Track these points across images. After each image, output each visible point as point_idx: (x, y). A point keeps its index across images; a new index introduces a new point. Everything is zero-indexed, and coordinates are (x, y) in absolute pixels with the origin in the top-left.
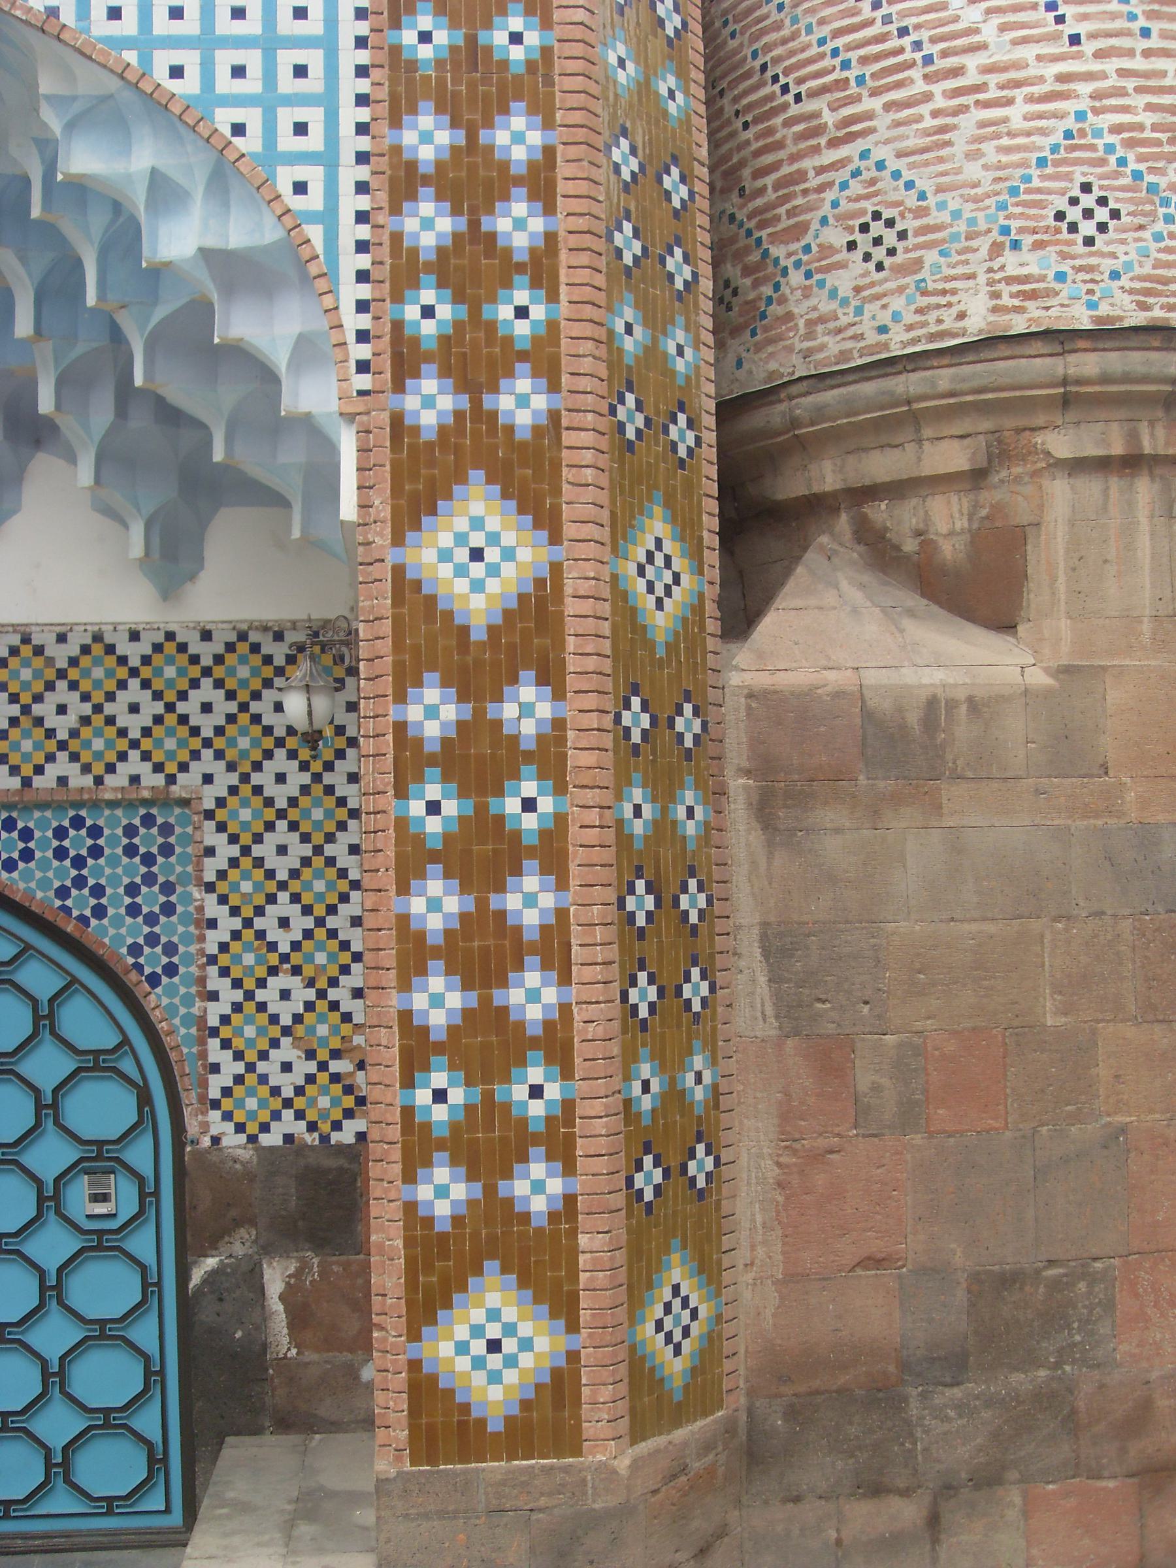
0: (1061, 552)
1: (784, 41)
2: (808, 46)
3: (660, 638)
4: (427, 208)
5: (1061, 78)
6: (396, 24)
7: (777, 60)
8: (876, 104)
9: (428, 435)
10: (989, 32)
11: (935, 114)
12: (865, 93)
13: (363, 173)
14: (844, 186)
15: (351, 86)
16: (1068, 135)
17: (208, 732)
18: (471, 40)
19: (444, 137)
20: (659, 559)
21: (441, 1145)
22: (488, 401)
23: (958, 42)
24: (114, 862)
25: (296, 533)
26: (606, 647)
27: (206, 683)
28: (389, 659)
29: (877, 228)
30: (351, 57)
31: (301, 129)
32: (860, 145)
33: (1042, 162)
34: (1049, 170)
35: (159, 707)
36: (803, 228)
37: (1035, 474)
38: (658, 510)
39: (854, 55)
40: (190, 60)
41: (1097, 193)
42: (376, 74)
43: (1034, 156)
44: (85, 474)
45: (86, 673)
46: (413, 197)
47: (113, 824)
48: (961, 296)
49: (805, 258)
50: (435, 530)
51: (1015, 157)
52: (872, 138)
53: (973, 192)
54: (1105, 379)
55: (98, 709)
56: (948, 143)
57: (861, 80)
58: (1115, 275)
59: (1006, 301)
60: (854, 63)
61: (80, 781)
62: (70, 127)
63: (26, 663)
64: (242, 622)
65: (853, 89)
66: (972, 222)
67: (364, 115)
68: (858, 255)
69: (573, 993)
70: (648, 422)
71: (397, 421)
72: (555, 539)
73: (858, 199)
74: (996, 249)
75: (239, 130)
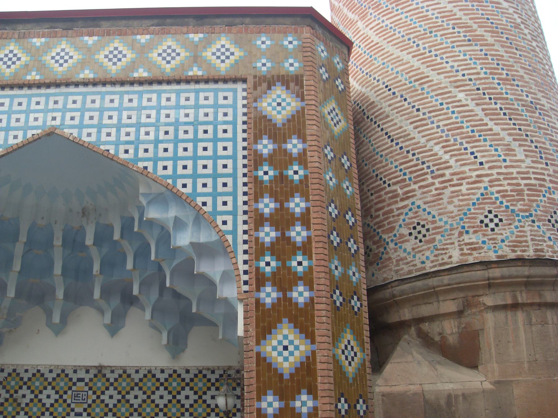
0: (492, 339)
1: (383, 167)
2: (391, 168)
3: (351, 376)
4: (267, 229)
5: (478, 176)
6: (256, 169)
7: (381, 173)
8: (416, 187)
9: (268, 306)
10: (452, 162)
11: (436, 189)
12: (412, 183)
13: (246, 217)
14: (407, 214)
16: (482, 194)
17: (187, 406)
18: (281, 174)
19: (272, 205)
20: (349, 348)
22: (289, 294)
23: (442, 166)
25: (220, 337)
26: (332, 380)
27: (187, 388)
28: (255, 386)
29: (419, 228)
31: (225, 203)
32: (411, 200)
33: (474, 204)
34: (477, 206)
36: (393, 228)
37: (481, 311)
38: (348, 330)
39: (407, 171)
41: (494, 213)
42: (250, 185)
43: (471, 202)
44: (148, 315)
45: (145, 384)
46: (263, 225)
48: (450, 250)
49: (394, 239)
50: (271, 339)
51: (465, 203)
52: (415, 198)
53: (451, 215)
54: (503, 277)
55: (149, 397)
56: (442, 199)
57: (410, 179)
58: (503, 241)
59: (465, 251)
60: (407, 173)
62: (149, 203)
63: (124, 380)
64: (200, 367)
65: (408, 182)
66: (451, 225)
67: (246, 198)
68: (413, 237)
70: (344, 299)
71: (258, 301)
72: (313, 342)
73: (412, 218)
74: (461, 234)
75: (204, 204)
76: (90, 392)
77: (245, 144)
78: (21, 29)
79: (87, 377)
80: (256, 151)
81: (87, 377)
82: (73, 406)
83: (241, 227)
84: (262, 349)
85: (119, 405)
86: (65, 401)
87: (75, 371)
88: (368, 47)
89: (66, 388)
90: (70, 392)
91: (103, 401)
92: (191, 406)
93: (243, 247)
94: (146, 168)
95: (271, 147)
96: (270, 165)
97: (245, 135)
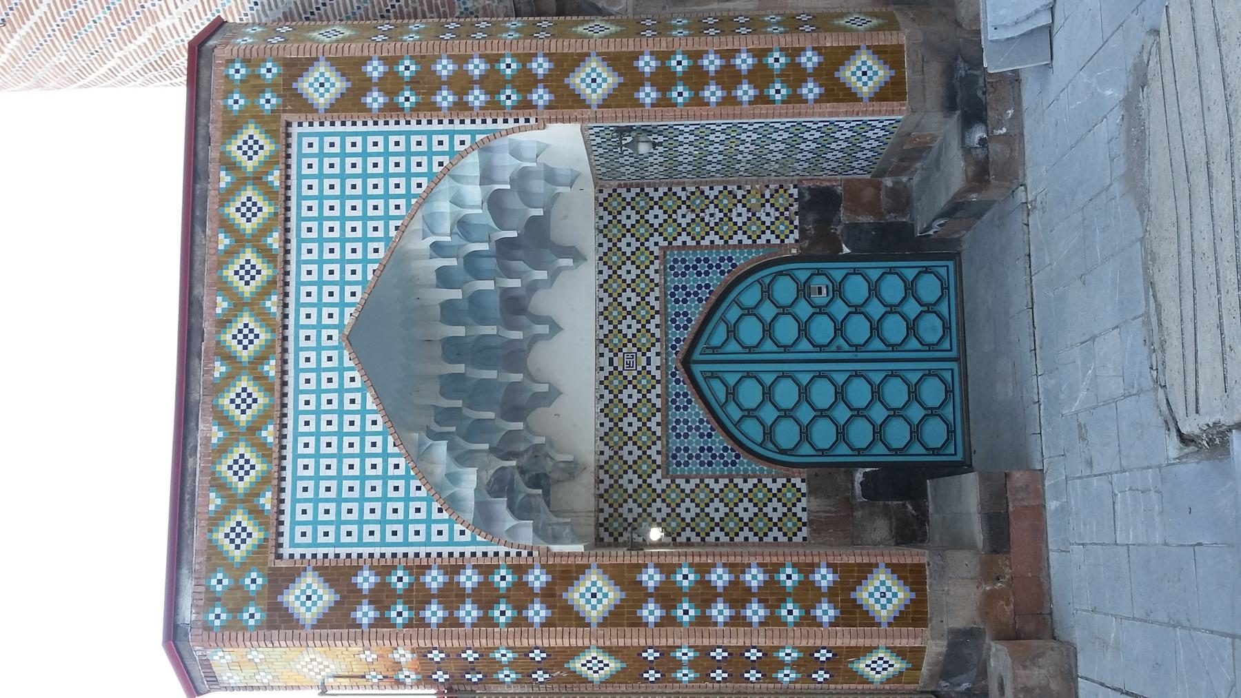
1: (373, 6)
3: (619, 29)
6: (403, 109)
7: (380, 11)
13: (457, 121)
15: (424, 126)
21: (795, 91)
24: (688, 281)
30: (414, 126)
35: (629, 262)
40: (414, 181)
46: (467, 103)
47: (673, 281)
61: (657, 292)
67: (435, 121)
69: (743, 48)
72: (588, 55)
76: (625, 350)
77: (370, 123)
78: (198, 393)
79: (608, 355)
80: (380, 110)
81: (608, 355)
82: (639, 368)
83: (468, 126)
84: (594, 103)
85: (638, 317)
86: (634, 377)
87: (602, 369)
88: (202, 14)
89: (621, 378)
90: (625, 373)
91: (634, 336)
92: (638, 240)
93: (490, 125)
94: (397, 228)
95: (375, 94)
96: (397, 94)
97: (359, 123)
